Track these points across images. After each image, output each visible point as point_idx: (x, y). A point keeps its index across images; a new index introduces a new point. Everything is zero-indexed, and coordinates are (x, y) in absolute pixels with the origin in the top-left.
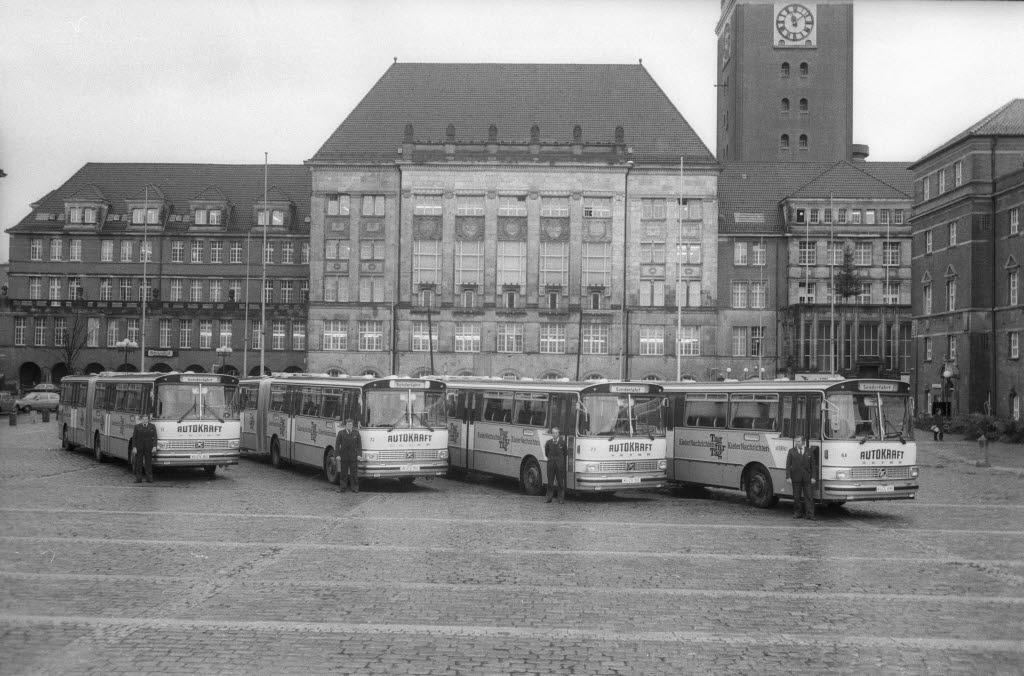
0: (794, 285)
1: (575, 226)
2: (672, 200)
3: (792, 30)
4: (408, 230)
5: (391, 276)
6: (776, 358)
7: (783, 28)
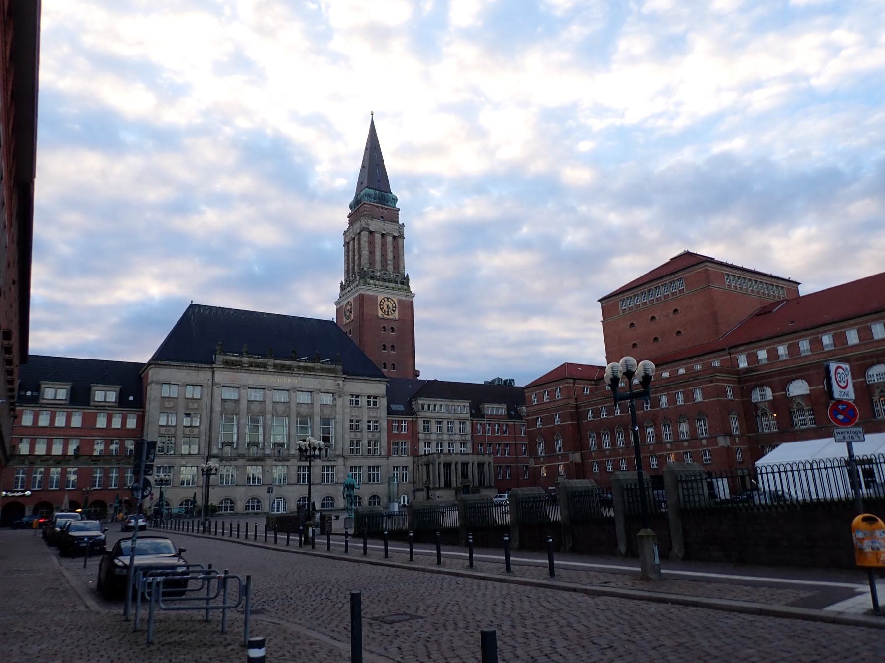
0: (421, 444)
4: (217, 408)
5: (204, 438)
6: (414, 483)
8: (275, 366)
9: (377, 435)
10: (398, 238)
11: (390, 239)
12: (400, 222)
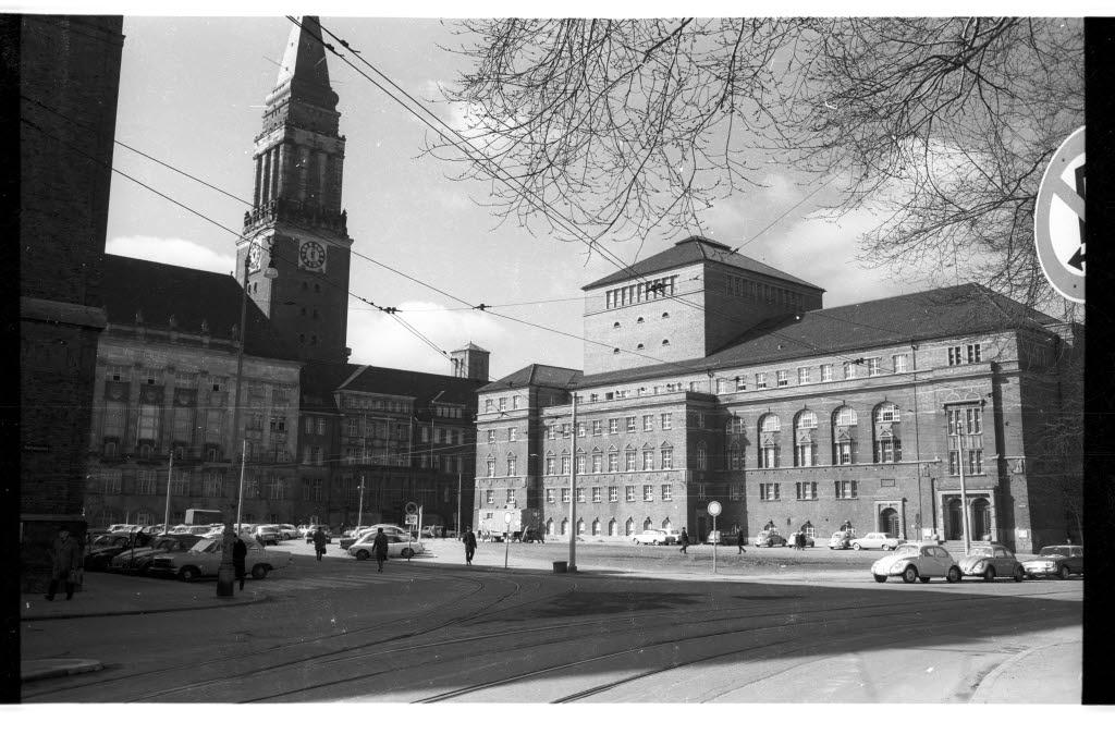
1: (201, 397)
2: (270, 383)
3: (310, 259)
7: (305, 257)
8: (147, 336)
9: (283, 435)
10: (337, 155)
11: (323, 158)
12: (340, 134)
